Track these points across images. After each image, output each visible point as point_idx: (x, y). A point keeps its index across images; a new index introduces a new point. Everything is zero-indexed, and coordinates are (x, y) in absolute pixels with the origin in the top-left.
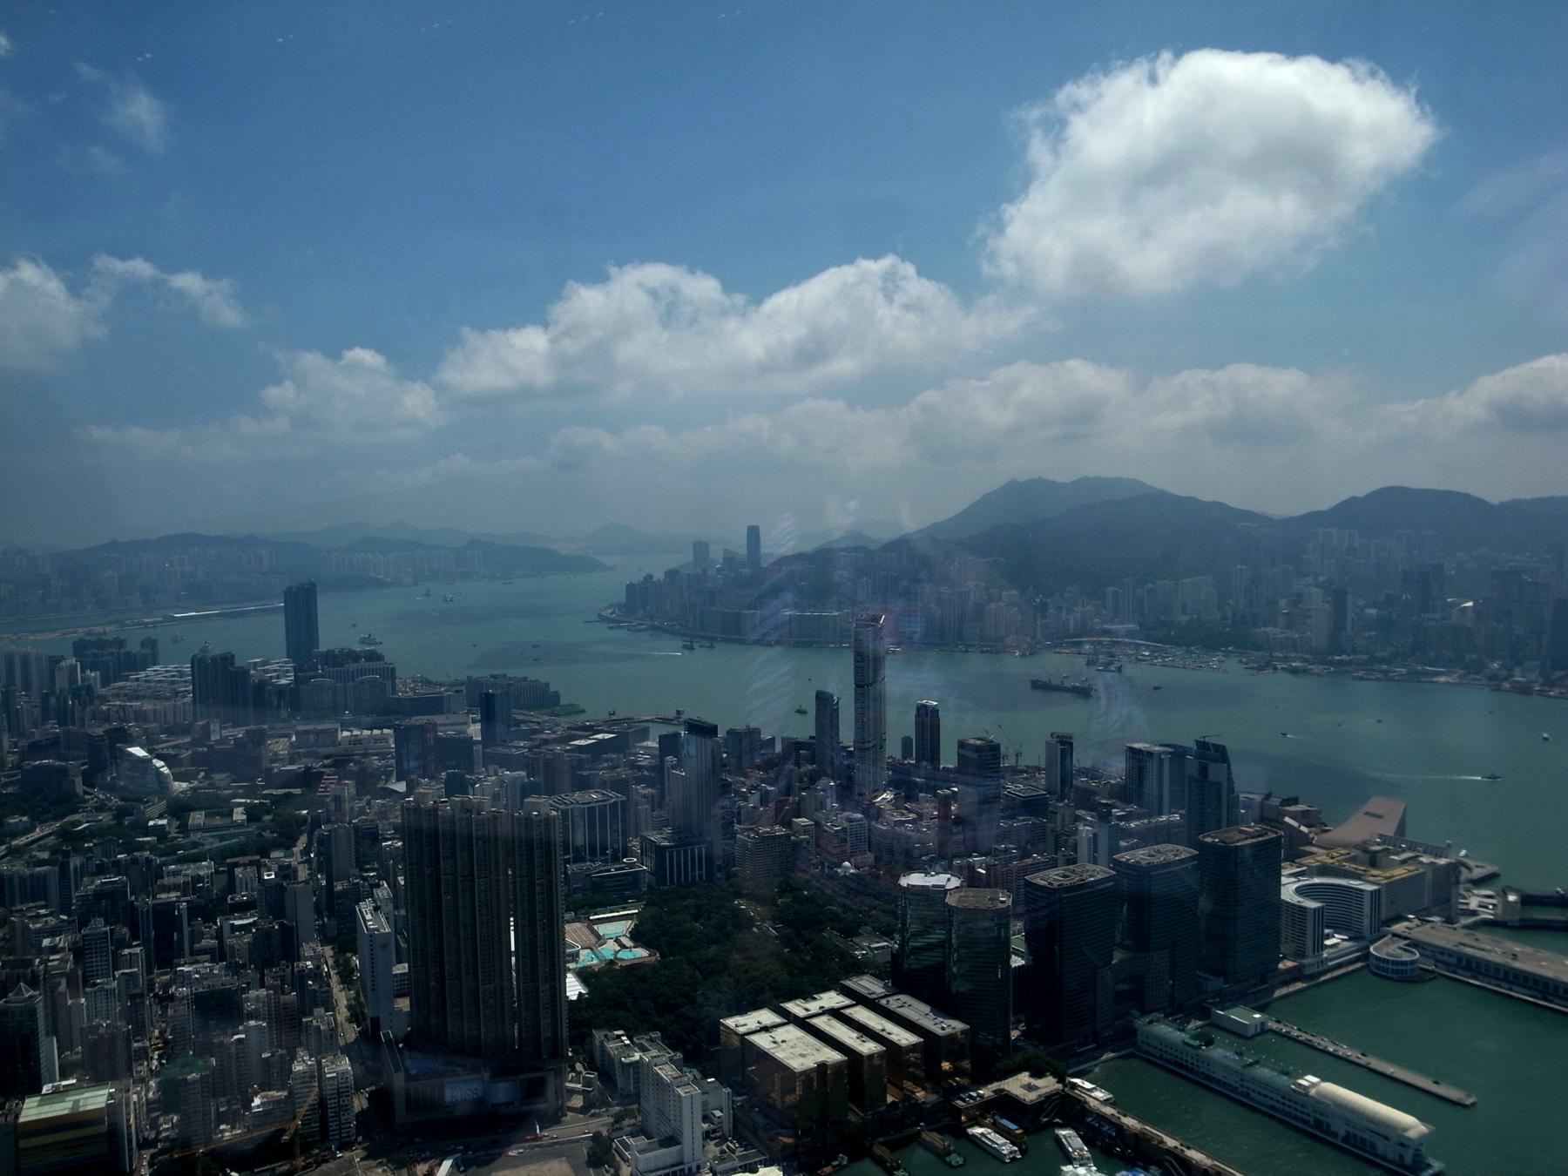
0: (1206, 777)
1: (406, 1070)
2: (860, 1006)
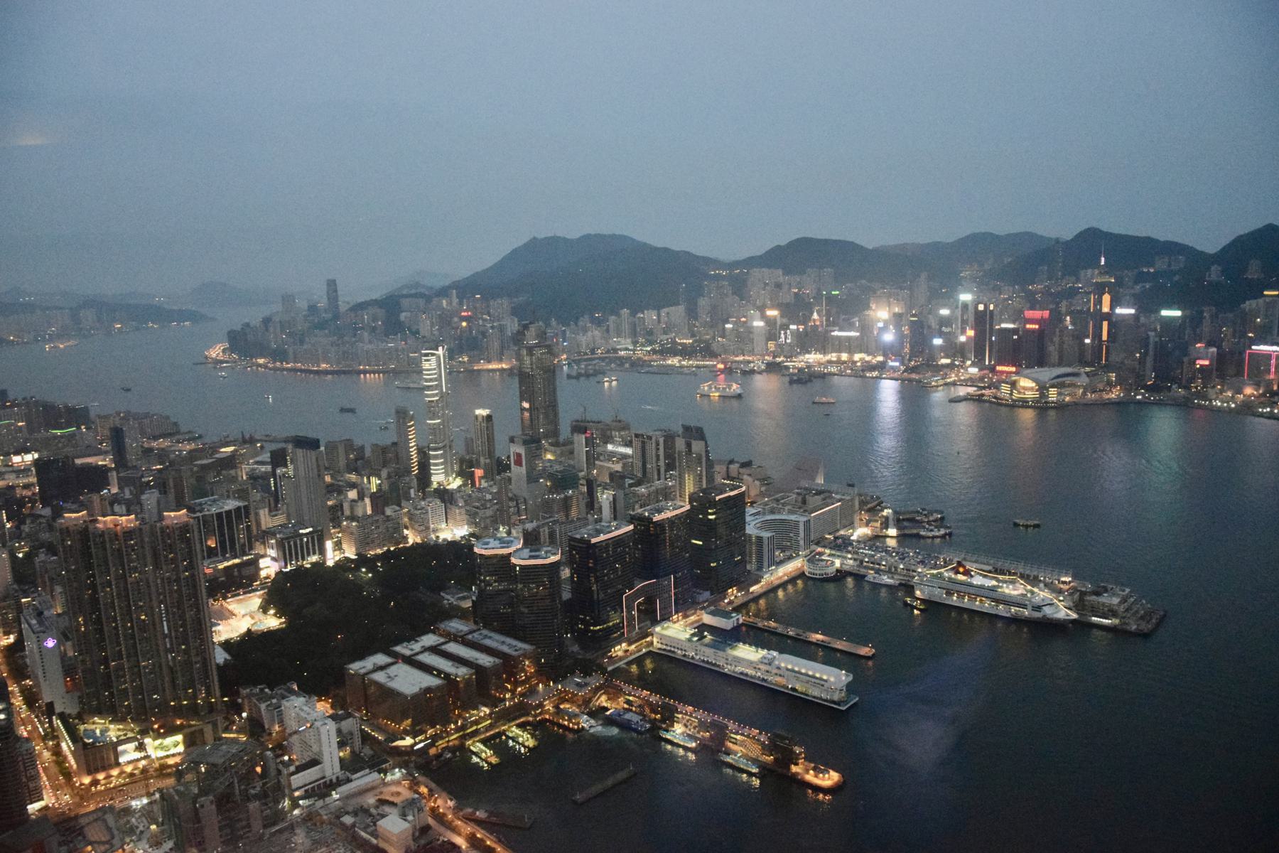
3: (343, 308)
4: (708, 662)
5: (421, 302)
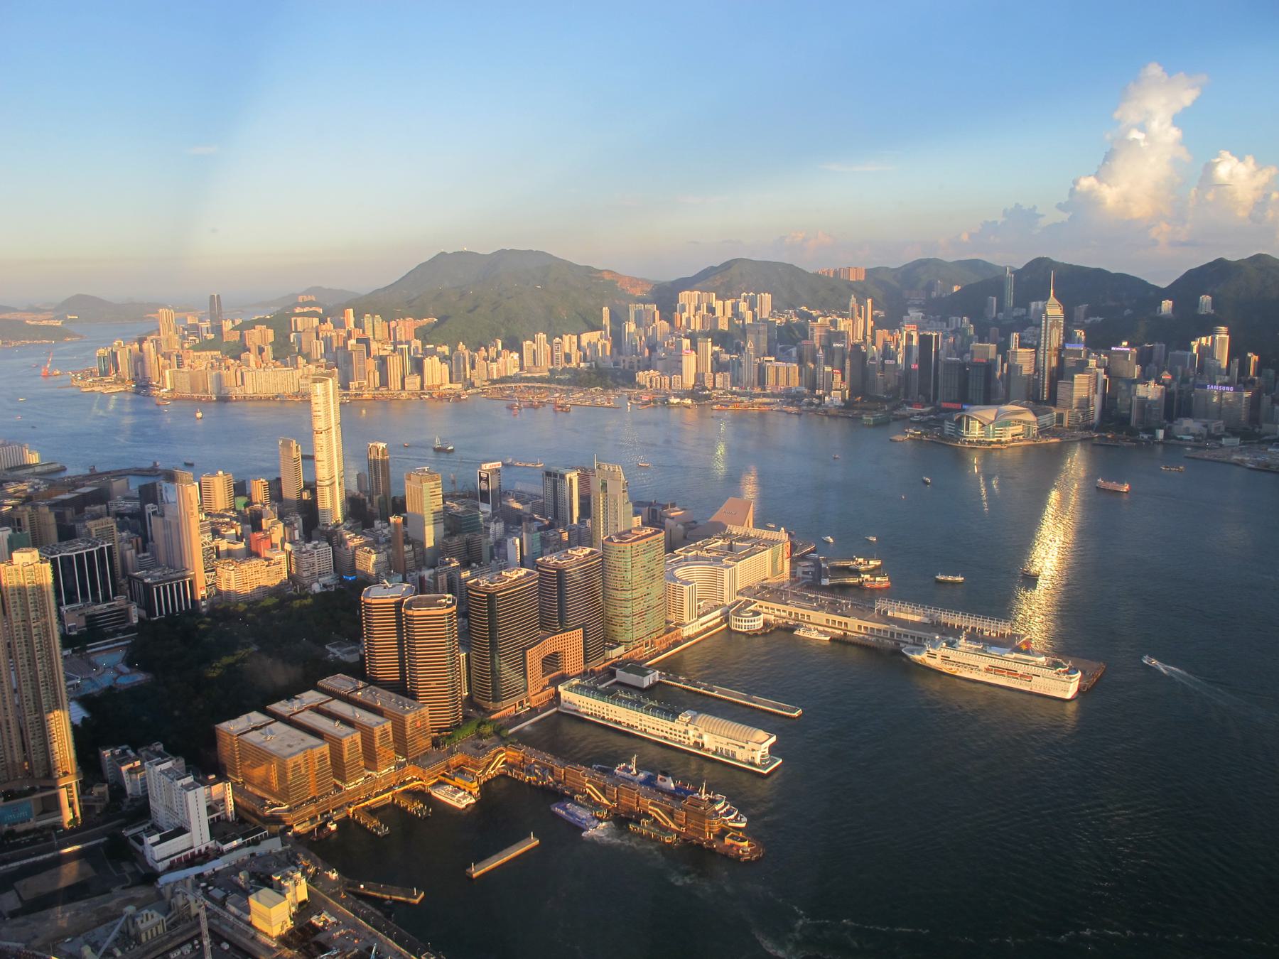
2: (335, 701)
3: (228, 325)
4: (620, 723)
5: (316, 321)
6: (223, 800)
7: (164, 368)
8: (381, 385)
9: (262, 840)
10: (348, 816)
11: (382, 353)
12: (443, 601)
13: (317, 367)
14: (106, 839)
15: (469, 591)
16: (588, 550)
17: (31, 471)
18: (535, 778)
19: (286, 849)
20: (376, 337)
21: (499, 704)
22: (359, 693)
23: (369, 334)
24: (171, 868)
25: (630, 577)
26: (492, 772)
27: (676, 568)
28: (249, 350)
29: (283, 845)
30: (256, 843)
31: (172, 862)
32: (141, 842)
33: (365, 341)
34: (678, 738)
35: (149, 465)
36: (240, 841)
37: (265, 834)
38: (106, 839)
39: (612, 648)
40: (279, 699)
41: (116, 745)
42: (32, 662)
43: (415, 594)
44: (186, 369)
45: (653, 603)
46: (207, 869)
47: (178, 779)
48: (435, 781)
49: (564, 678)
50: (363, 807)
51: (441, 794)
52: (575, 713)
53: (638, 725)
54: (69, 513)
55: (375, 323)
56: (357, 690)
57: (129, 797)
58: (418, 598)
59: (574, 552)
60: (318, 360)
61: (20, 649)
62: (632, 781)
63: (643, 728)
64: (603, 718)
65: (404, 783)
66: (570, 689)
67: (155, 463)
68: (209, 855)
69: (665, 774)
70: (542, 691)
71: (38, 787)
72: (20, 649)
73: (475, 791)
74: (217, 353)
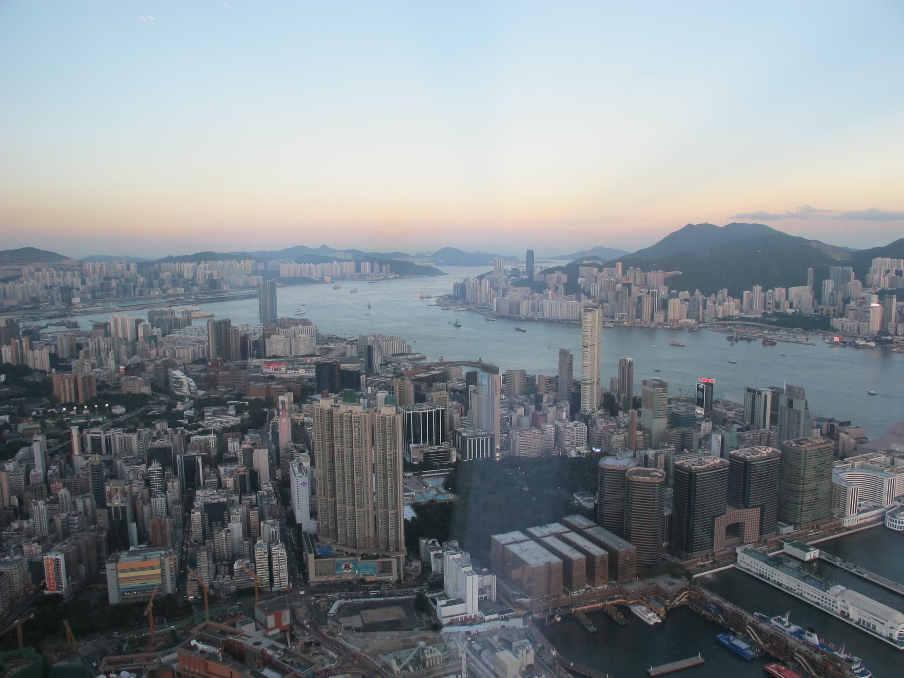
0: (791, 407)
1: (315, 553)
3: (537, 271)
4: (781, 584)
5: (595, 270)
6: (490, 587)
7: (494, 297)
8: (637, 317)
9: (511, 618)
10: (570, 614)
11: (639, 294)
12: (656, 473)
13: (593, 302)
14: (415, 596)
15: (676, 469)
16: (770, 450)
17: (405, 357)
18: (709, 614)
19: (525, 628)
20: (637, 283)
21: (689, 554)
22: (590, 530)
23: (631, 281)
24: (451, 624)
25: (802, 475)
26: (677, 603)
27: (842, 472)
28: (549, 288)
29: (524, 625)
30: (506, 619)
31: (452, 620)
32: (435, 603)
33: (629, 286)
34: (828, 605)
35: (476, 359)
36: (496, 616)
37: (514, 615)
38: (415, 596)
39: (785, 527)
40: (534, 524)
41: (430, 538)
42: (385, 477)
43: (636, 466)
44: (507, 298)
45: (820, 496)
46: (473, 629)
47: (463, 567)
48: (636, 601)
49: (742, 543)
50: (581, 610)
51: (640, 611)
52: (749, 572)
53: (796, 589)
54: (424, 386)
55: (637, 274)
56: (589, 527)
57: (433, 572)
58: (638, 470)
59: (759, 450)
60: (594, 297)
61: (379, 467)
62: (784, 630)
63: (800, 592)
64: (769, 579)
65: (613, 599)
66: (746, 552)
67: (480, 359)
68: (475, 620)
69: (812, 631)
70: (724, 550)
71: (381, 555)
72: (379, 467)
73: (662, 615)
74: (528, 289)
